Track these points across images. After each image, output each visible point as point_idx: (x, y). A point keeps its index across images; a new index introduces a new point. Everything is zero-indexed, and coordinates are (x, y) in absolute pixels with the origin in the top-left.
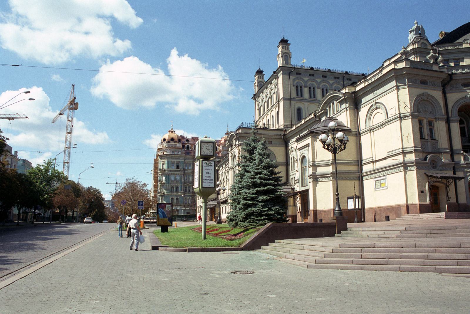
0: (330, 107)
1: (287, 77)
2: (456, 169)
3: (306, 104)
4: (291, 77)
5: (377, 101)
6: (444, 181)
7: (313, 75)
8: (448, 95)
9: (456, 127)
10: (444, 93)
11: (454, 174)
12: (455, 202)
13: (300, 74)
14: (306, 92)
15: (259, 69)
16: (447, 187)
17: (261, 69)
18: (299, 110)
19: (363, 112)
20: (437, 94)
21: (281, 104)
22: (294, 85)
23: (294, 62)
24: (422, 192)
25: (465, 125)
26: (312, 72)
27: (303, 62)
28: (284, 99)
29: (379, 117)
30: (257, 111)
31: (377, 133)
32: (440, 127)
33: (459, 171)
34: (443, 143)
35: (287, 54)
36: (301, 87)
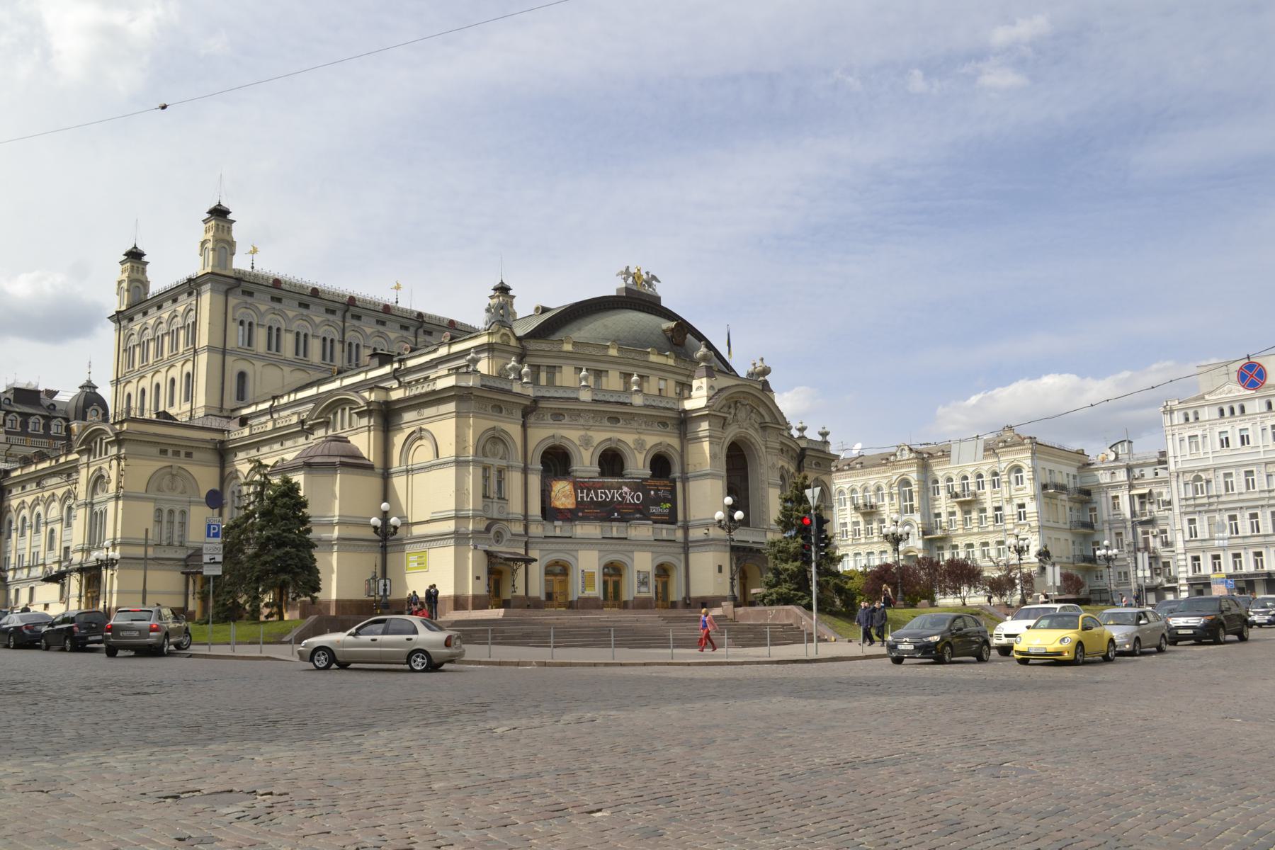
0: (335, 414)
1: (221, 298)
3: (259, 364)
4: (230, 298)
7: (279, 300)
8: (530, 431)
9: (535, 481)
10: (524, 426)
13: (251, 294)
16: (514, 571)
17: (140, 247)
18: (242, 376)
19: (399, 440)
20: (514, 430)
21: (203, 359)
22: (234, 320)
23: (240, 262)
24: (478, 578)
26: (277, 289)
28: (210, 348)
29: (422, 453)
31: (418, 478)
32: (515, 479)
34: (516, 507)
36: (250, 324)
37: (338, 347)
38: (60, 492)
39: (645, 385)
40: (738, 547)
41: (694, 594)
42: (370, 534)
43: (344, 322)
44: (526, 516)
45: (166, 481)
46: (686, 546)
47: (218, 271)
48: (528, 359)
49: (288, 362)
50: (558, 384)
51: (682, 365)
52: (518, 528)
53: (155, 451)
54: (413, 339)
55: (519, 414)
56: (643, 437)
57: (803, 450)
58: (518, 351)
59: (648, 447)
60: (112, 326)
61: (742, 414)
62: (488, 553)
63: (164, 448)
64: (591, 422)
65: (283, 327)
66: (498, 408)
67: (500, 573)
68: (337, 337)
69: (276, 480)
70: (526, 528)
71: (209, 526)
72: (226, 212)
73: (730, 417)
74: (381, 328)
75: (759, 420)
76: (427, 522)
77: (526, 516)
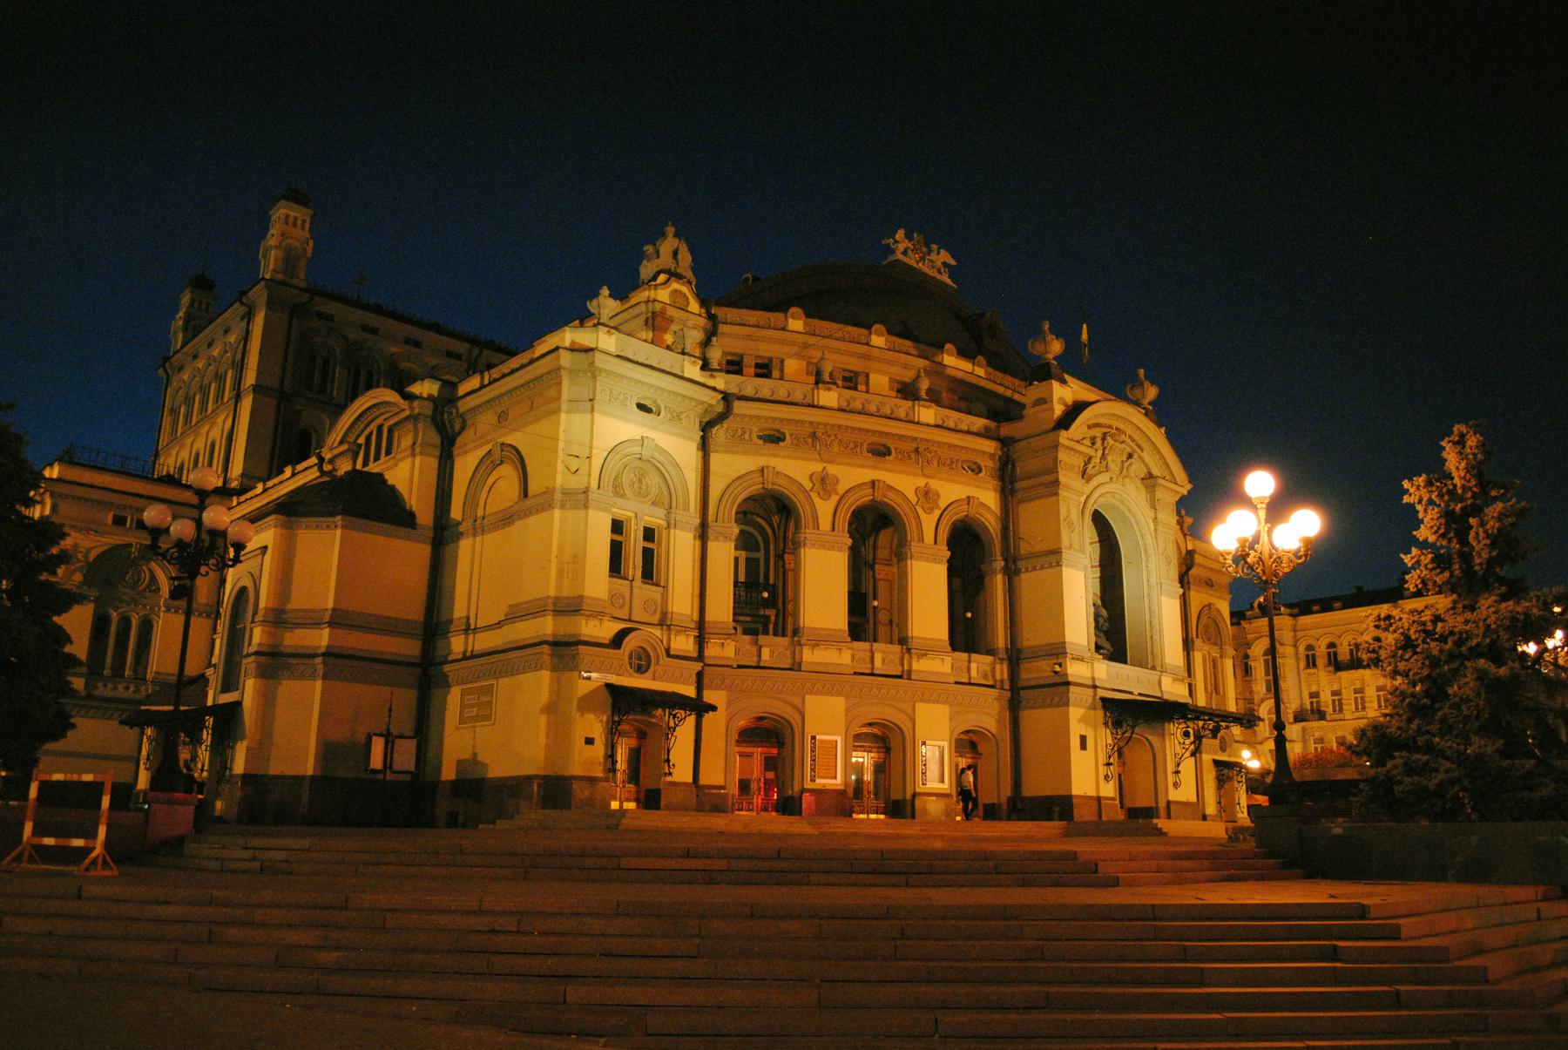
2: (706, 681)
5: (508, 440)
8: (715, 459)
10: (704, 446)
11: (699, 689)
12: (690, 780)
20: (682, 450)
24: (590, 741)
25: (760, 555)
28: (257, 388)
30: (167, 420)
33: (718, 688)
36: (326, 362)
44: (701, 624)
52: (684, 644)
59: (943, 504)
70: (701, 641)
76: (499, 625)
77: (701, 624)
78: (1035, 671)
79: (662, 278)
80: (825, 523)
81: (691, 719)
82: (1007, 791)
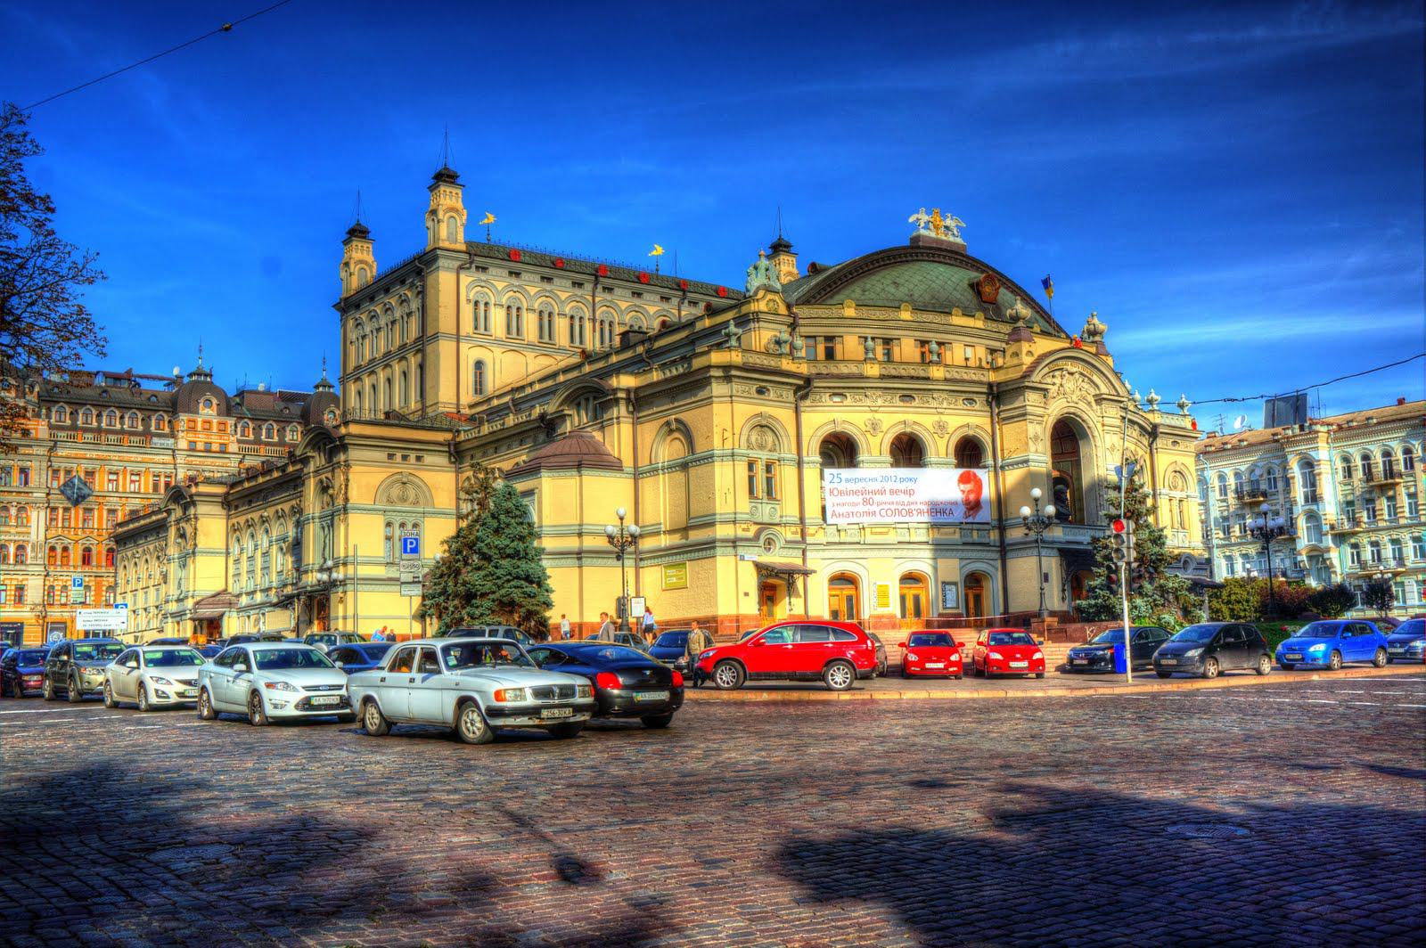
1: (453, 276)
3: (498, 351)
4: (462, 276)
6: (786, 576)
7: (517, 274)
8: (804, 417)
10: (797, 411)
13: (484, 269)
14: (498, 318)
15: (359, 225)
18: (479, 365)
20: (784, 415)
22: (469, 301)
24: (746, 594)
27: (486, 221)
34: (790, 509)
35: (454, 215)
37: (588, 326)
38: (287, 507)
39: (948, 354)
40: (1069, 550)
41: (1015, 608)
42: (601, 543)
43: (594, 296)
45: (396, 491)
46: (1004, 550)
47: (446, 245)
48: (797, 330)
49: (530, 345)
50: (838, 355)
51: (992, 326)
52: (790, 534)
53: (381, 455)
54: (676, 312)
55: (791, 398)
56: (944, 418)
57: (1155, 427)
58: (791, 320)
59: (950, 431)
60: (338, 314)
61: (1069, 384)
62: (759, 567)
63: (392, 448)
64: (880, 402)
65: (525, 305)
66: (760, 391)
67: (773, 588)
68: (587, 314)
69: (499, 484)
70: (803, 534)
71: (405, 540)
72: (457, 177)
73: (1053, 389)
74: (637, 301)
75: (1093, 391)
77: (802, 519)
78: (1015, 534)
79: (761, 293)
80: (875, 452)
81: (801, 579)
82: (1001, 609)
